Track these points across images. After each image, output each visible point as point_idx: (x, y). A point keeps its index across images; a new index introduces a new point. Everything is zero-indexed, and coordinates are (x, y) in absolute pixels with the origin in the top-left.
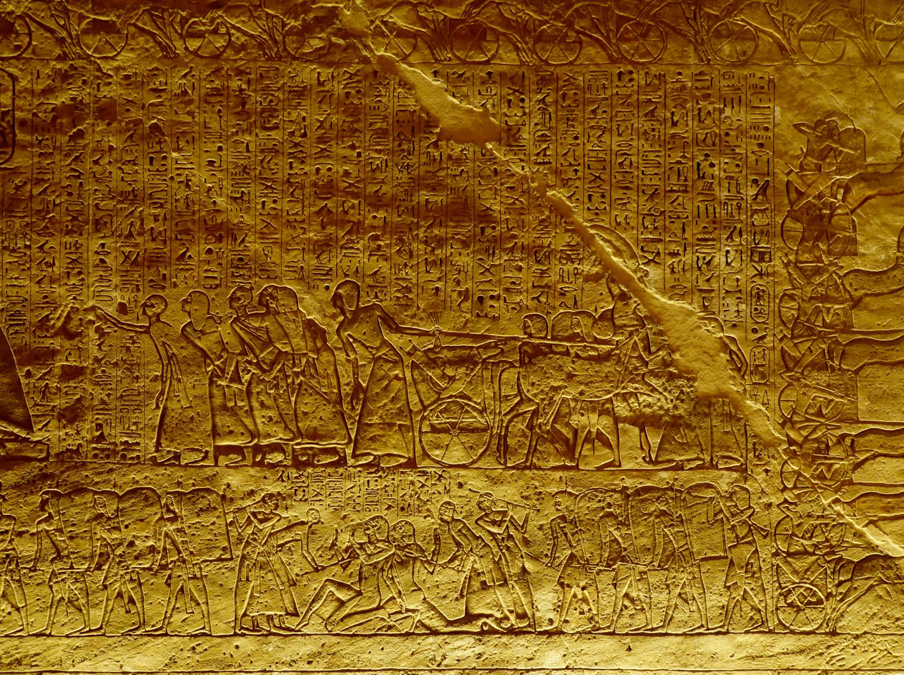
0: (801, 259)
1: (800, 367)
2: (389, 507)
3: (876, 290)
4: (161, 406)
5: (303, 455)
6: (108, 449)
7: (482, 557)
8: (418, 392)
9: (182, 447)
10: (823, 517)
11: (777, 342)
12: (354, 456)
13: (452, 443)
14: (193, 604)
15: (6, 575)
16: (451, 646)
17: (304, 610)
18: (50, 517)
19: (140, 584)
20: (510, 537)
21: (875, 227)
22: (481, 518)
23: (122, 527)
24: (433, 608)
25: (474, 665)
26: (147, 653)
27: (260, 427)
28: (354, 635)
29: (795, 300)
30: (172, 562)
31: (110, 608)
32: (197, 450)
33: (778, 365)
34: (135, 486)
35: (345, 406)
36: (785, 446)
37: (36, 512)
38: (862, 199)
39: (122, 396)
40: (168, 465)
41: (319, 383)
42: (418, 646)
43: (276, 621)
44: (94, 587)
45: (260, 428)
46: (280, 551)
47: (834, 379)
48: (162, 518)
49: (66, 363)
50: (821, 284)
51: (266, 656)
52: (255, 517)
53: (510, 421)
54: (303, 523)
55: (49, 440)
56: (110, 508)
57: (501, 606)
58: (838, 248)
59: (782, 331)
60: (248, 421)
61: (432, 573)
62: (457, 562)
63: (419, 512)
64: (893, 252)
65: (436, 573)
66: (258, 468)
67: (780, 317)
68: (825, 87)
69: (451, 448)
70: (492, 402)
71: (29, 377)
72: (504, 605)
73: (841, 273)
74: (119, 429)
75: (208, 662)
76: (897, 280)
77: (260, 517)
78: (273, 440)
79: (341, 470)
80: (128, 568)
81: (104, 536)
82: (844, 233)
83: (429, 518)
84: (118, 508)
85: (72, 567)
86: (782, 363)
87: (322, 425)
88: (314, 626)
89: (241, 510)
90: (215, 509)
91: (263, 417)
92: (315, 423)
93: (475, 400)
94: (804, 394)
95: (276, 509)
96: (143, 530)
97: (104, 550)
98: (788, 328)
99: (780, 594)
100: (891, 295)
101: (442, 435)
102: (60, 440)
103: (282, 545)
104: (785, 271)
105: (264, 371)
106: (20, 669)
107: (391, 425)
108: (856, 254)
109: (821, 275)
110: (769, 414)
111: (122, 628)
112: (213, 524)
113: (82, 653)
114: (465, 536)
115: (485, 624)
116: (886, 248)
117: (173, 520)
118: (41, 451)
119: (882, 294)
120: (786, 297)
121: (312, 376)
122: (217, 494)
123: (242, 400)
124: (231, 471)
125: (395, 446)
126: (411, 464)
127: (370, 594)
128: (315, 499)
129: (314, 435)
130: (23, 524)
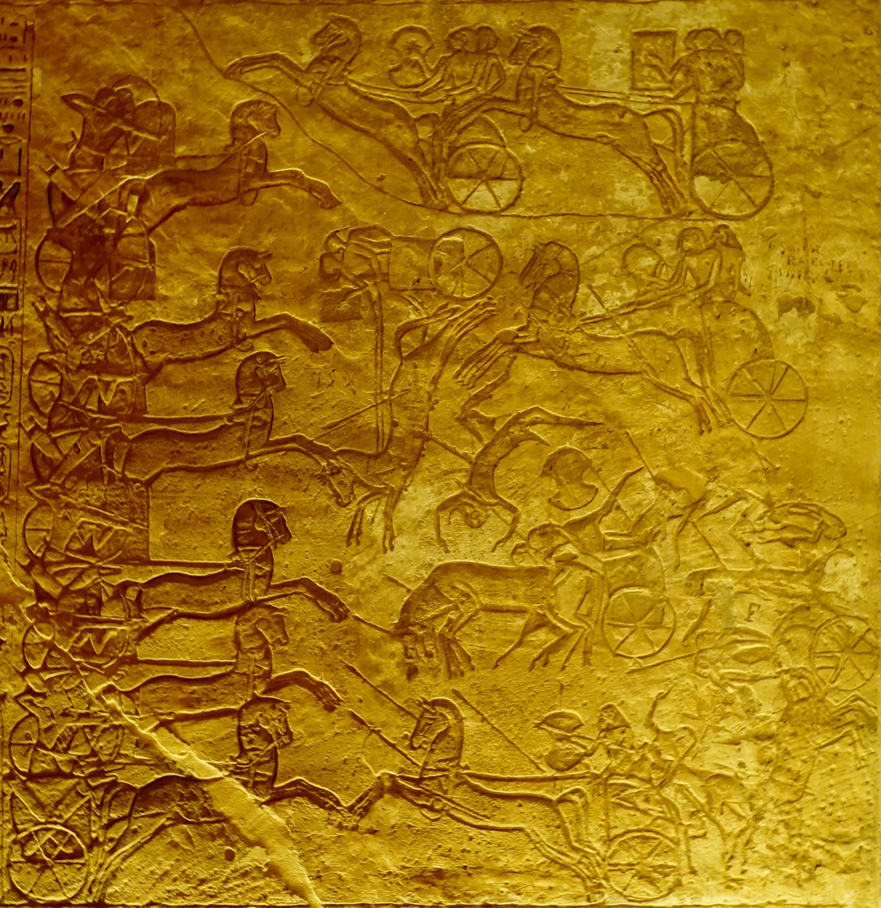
0: (67, 305)
1: (59, 477)
3: (184, 353)
10: (87, 716)
11: (23, 436)
21: (184, 255)
29: (55, 370)
33: (23, 472)
36: (30, 603)
38: (167, 211)
47: (113, 495)
50: (97, 345)
58: (125, 288)
59: (31, 419)
64: (210, 294)
67: (31, 397)
68: (115, 38)
73: (131, 326)
76: (216, 338)
82: (136, 264)
86: (31, 470)
94: (65, 518)
98: (41, 414)
99: (15, 842)
100: (206, 362)
104: (41, 324)
108: (152, 298)
109: (97, 330)
110: (6, 552)
116: (199, 287)
119: (191, 360)
120: (41, 366)
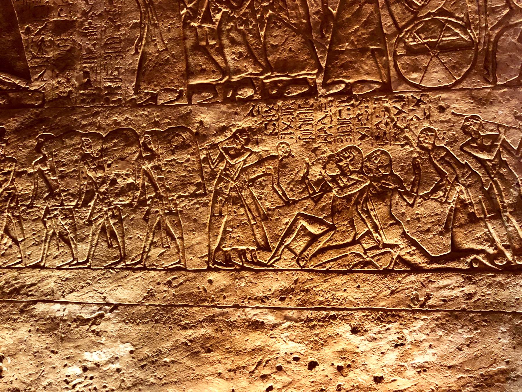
2: (363, 137)
4: (140, 51)
5: (273, 89)
6: (93, 94)
7: (469, 186)
8: (391, 14)
9: (158, 89)
12: (325, 85)
13: (431, 65)
14: (169, 239)
15: (8, 212)
16: (435, 285)
17: (276, 245)
18: (45, 158)
19: (121, 220)
20: (504, 164)
22: (467, 144)
23: (105, 166)
24: (412, 243)
25: (464, 306)
26: (129, 285)
27: (231, 63)
28: (328, 272)
30: (150, 198)
31: (95, 242)
32: (172, 90)
34: (118, 127)
35: (314, 35)
37: (33, 154)
39: (106, 44)
40: (146, 106)
41: (287, 14)
42: (398, 285)
43: (248, 256)
44: (81, 222)
45: (231, 65)
46: (251, 186)
48: (140, 156)
49: (59, 19)
51: (238, 292)
52: (228, 153)
53: (499, 36)
54: (274, 157)
55: (44, 89)
56: (95, 150)
57: (494, 241)
60: (218, 59)
61: (412, 205)
62: (441, 193)
63: (397, 140)
65: (416, 205)
66: (229, 105)
69: (431, 70)
70: (477, 16)
71: (28, 33)
72: (497, 240)
74: (103, 75)
75: (183, 297)
77: (232, 152)
78: (243, 75)
79: (311, 101)
80: (111, 205)
81: (90, 174)
83: (407, 147)
84: (102, 148)
85: (62, 204)
87: (291, 57)
88: (286, 262)
89: (214, 146)
90: (189, 146)
91: (234, 53)
92: (285, 55)
93: (457, 15)
95: (247, 144)
96: (124, 168)
97: (90, 188)
101: (420, 57)
102: (54, 88)
103: (254, 180)
105: (233, 8)
106: (19, 298)
107: (363, 51)
111: (105, 262)
112: (188, 160)
113: (71, 285)
114: (449, 164)
115: (475, 260)
117: (150, 159)
118: (37, 99)
121: (281, 9)
122: (191, 132)
123: (213, 39)
124: (204, 109)
125: (368, 72)
126: (386, 89)
127: (344, 229)
128: (285, 132)
129: (283, 67)
130: (23, 165)
